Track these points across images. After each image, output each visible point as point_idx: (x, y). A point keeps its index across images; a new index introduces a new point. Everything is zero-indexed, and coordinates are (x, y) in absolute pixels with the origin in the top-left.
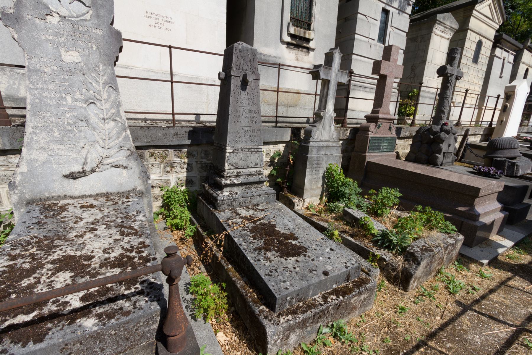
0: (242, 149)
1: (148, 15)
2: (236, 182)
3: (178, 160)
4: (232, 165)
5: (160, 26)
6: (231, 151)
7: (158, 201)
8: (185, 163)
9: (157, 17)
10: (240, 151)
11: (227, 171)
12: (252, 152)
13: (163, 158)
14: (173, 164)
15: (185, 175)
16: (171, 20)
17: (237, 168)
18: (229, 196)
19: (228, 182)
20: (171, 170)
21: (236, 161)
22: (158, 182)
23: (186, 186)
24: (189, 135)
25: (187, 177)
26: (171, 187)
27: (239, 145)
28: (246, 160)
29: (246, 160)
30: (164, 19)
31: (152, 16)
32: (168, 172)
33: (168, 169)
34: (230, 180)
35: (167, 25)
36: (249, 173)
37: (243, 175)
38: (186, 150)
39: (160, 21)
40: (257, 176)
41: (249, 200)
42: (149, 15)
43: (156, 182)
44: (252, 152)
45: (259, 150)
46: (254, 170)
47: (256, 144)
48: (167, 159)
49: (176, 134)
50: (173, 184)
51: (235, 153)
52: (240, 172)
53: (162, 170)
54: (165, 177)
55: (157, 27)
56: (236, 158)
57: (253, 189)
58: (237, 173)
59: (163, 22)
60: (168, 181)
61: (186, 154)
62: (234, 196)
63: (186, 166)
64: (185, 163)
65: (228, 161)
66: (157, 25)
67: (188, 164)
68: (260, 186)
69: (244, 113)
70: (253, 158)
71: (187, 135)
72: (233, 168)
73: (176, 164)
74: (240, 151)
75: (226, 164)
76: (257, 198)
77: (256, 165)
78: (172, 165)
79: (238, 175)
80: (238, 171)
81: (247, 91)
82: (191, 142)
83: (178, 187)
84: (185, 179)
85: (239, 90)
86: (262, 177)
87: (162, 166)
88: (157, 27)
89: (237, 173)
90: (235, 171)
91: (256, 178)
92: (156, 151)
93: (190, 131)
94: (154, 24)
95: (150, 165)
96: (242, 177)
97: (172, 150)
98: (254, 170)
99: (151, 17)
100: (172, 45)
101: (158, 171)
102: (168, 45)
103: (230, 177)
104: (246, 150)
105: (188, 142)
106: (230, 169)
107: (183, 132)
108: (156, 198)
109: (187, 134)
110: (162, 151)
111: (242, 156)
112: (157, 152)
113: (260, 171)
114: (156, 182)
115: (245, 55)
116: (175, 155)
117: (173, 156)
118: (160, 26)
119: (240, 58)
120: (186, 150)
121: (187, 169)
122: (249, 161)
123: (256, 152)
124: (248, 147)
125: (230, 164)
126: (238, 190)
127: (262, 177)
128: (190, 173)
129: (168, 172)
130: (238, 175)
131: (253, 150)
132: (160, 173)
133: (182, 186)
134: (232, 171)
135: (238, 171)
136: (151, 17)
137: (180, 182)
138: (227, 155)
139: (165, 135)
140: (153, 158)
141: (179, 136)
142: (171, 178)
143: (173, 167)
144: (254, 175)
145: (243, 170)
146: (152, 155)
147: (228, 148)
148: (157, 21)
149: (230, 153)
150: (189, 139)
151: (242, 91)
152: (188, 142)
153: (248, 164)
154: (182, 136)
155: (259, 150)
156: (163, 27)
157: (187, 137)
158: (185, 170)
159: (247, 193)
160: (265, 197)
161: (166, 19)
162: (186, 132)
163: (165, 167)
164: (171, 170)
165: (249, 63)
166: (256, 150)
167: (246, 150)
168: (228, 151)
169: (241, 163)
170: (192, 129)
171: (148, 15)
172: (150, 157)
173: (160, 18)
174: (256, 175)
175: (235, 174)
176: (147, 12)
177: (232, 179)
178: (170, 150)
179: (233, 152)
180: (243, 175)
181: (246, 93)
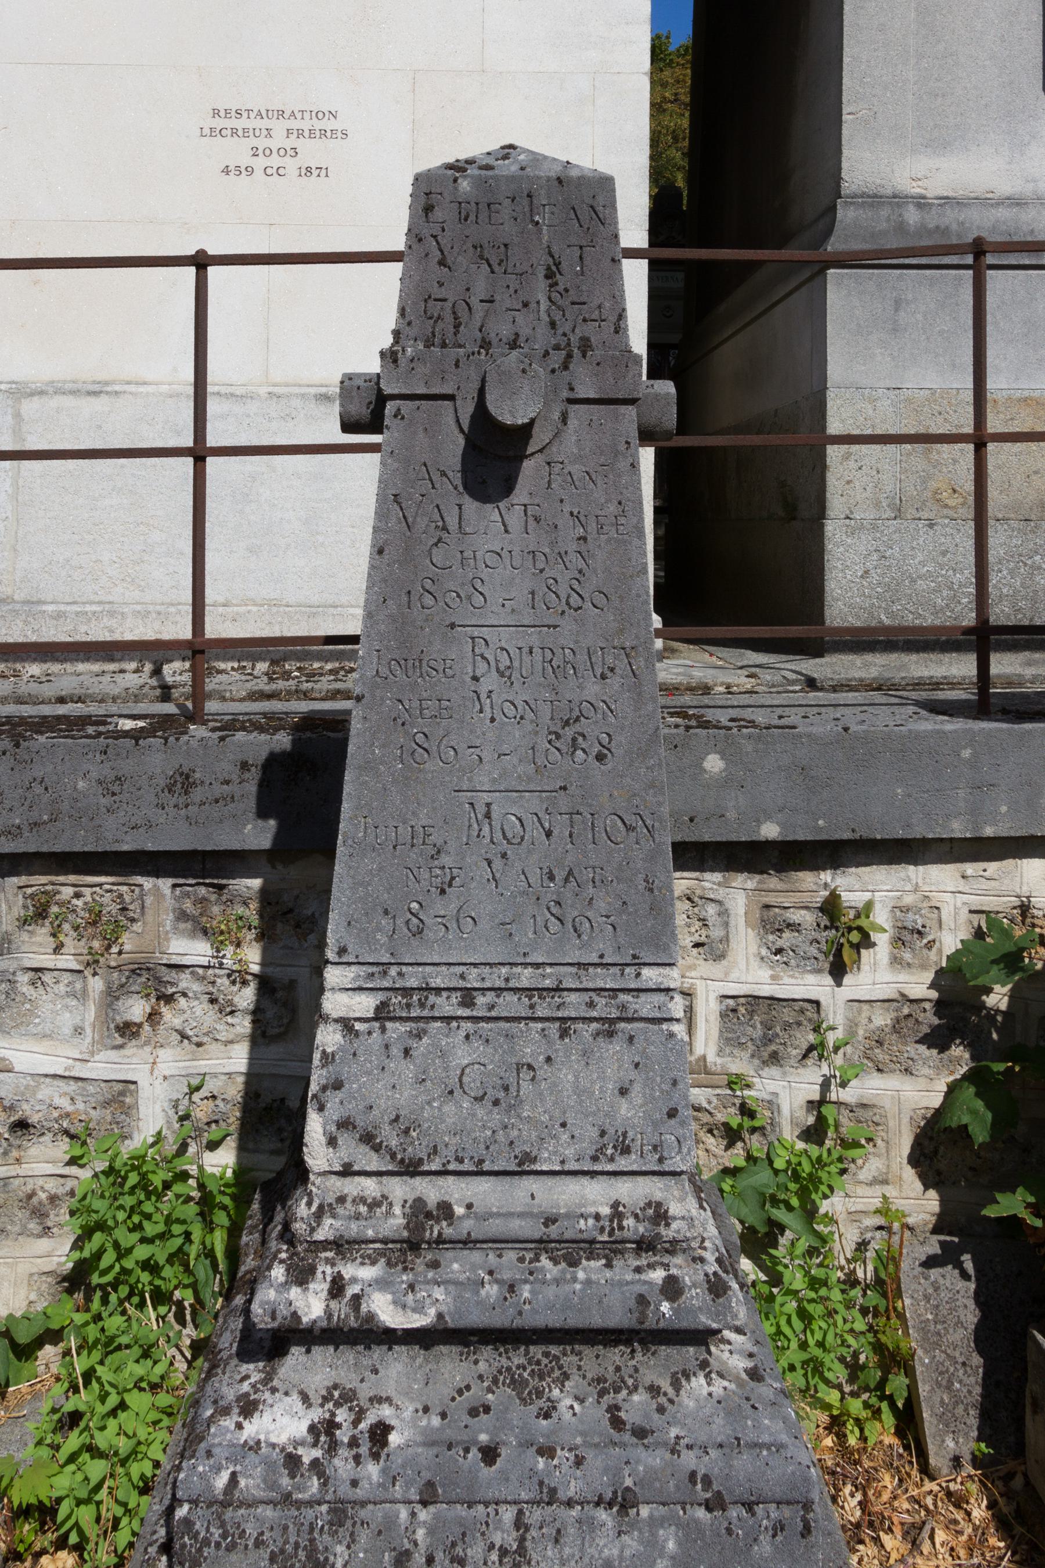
0: (468, 997)
1: (219, 123)
2: (385, 1310)
3: (195, 950)
4: (368, 1139)
5: (275, 161)
6: (364, 1004)
7: (46, 1231)
8: (238, 977)
9: (264, 123)
10: (447, 1005)
11: (322, 1188)
12: (565, 1026)
13: (104, 927)
14: (171, 975)
15: (237, 1059)
16: (329, 124)
17: (411, 1169)
18: (292, 1462)
19: (312, 1305)
20: (153, 1017)
21: (406, 1097)
22: (57, 1095)
23: (242, 1149)
24: (265, 785)
25: (253, 1078)
26: (129, 1148)
27: (442, 959)
28: (501, 1097)
29: (501, 1097)
30: (294, 124)
31: (240, 124)
32: (128, 1030)
33: (136, 1009)
34: (337, 1288)
35: (312, 152)
36: (537, 1230)
37: (467, 1242)
38: (256, 883)
39: (279, 140)
40: (623, 1270)
41: (505, 1536)
42: (225, 122)
43: (48, 1092)
44: (565, 1026)
45: (645, 1005)
46: (595, 1196)
47: (603, 945)
48: (128, 941)
49: (183, 782)
50: (152, 1119)
51: (396, 1030)
52: (445, 1210)
53: (91, 1013)
54: (107, 1065)
55: (259, 172)
56: (408, 1070)
57: (572, 1406)
58: (419, 1213)
59: (288, 144)
60: (121, 1096)
61: (251, 913)
62: (342, 1465)
63: (246, 997)
64: (238, 977)
65: (333, 1100)
66: (260, 163)
67: (265, 985)
68: (654, 1367)
69: (490, 682)
70: (584, 1084)
71: (252, 788)
72: (373, 1162)
73: (185, 981)
74: (447, 1005)
75: (315, 1126)
76: (587, 1525)
77: (607, 1157)
78: (157, 981)
79: (419, 1241)
80: (430, 1191)
81: (520, 494)
82: (277, 838)
83: (183, 1147)
84: (235, 1091)
85: (451, 495)
86: (672, 1288)
87: (96, 985)
88: (259, 172)
89: (419, 1213)
90: (400, 1190)
91: (600, 1289)
92: (66, 887)
93: (273, 762)
94: (246, 160)
95: (24, 978)
96: (456, 1265)
97: (165, 884)
98: (595, 1196)
99: (234, 132)
100: (213, 249)
101: (67, 1021)
102: (191, 251)
103: (341, 1246)
104: (511, 1004)
105: (259, 835)
106: (347, 1171)
107: (227, 767)
108: (39, 1214)
109: (254, 776)
110: (100, 889)
111: (462, 1055)
112: (67, 892)
113: (660, 1215)
114: (48, 1092)
115: (509, 230)
116: (182, 916)
117: (168, 920)
118: (275, 161)
119: (462, 261)
120: (256, 883)
121: (257, 1014)
122: (536, 1105)
123: (608, 1028)
124: (526, 977)
125: (345, 1124)
126: (406, 1398)
127: (672, 1288)
128: (275, 1051)
129: (128, 1030)
130: (419, 1241)
131: (574, 1004)
132: (78, 1031)
133: (213, 1146)
134: (370, 1187)
135: (430, 1191)
136: (234, 132)
137: (202, 1111)
138: (328, 1038)
139: (113, 786)
140: (42, 933)
141: (198, 794)
142: (138, 1072)
143: (169, 999)
144: (573, 1250)
145: (482, 1191)
146: (41, 914)
147: (333, 975)
148: (262, 143)
149: (346, 1024)
150: (263, 813)
151: (471, 505)
152: (259, 835)
153: (526, 1137)
154: (219, 790)
155: (645, 1005)
156: (291, 165)
157: (252, 803)
158: (244, 1025)
159: (490, 1454)
160: (689, 1532)
161: (306, 125)
162: (244, 766)
163: (113, 995)
164: (153, 1017)
165: (542, 284)
166: (603, 1008)
167: (511, 1004)
168: (334, 1004)
169: (453, 1121)
170: (283, 740)
171: (219, 123)
172: (25, 922)
173: (279, 127)
174: (611, 1250)
175: (395, 1223)
176: (216, 113)
177: (360, 1273)
178: (148, 883)
179: (382, 1014)
180: (467, 1242)
181: (515, 518)
